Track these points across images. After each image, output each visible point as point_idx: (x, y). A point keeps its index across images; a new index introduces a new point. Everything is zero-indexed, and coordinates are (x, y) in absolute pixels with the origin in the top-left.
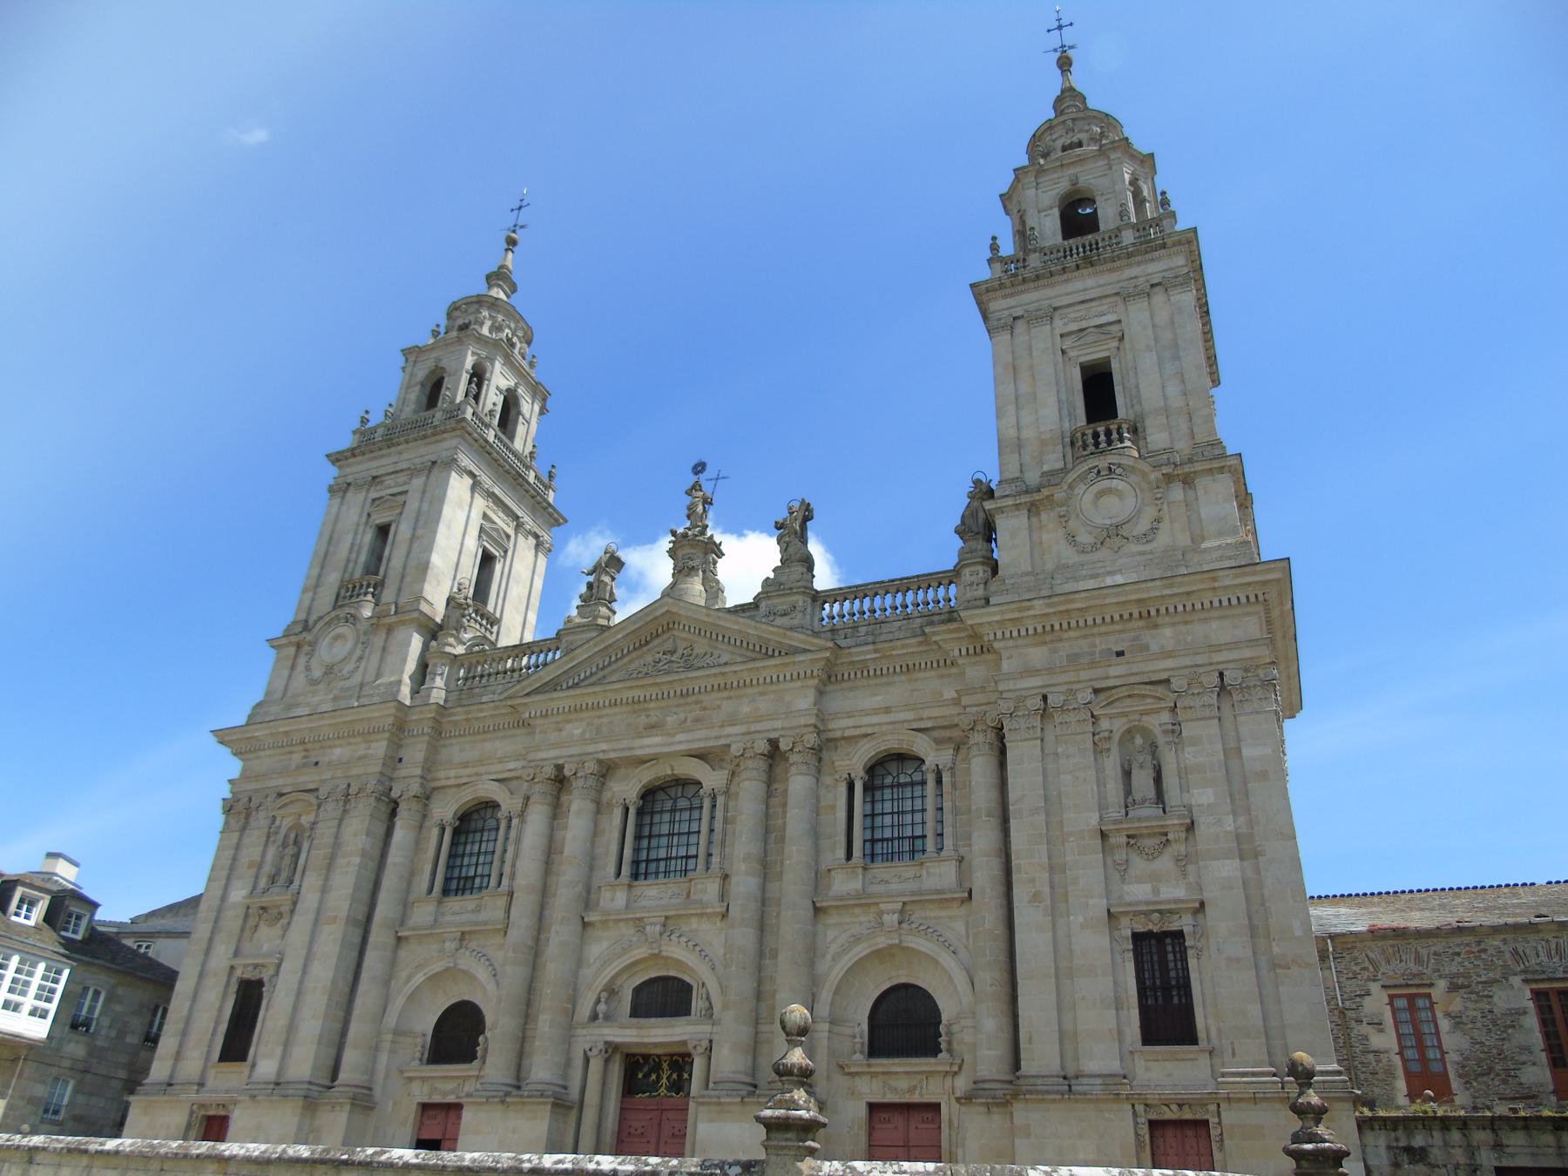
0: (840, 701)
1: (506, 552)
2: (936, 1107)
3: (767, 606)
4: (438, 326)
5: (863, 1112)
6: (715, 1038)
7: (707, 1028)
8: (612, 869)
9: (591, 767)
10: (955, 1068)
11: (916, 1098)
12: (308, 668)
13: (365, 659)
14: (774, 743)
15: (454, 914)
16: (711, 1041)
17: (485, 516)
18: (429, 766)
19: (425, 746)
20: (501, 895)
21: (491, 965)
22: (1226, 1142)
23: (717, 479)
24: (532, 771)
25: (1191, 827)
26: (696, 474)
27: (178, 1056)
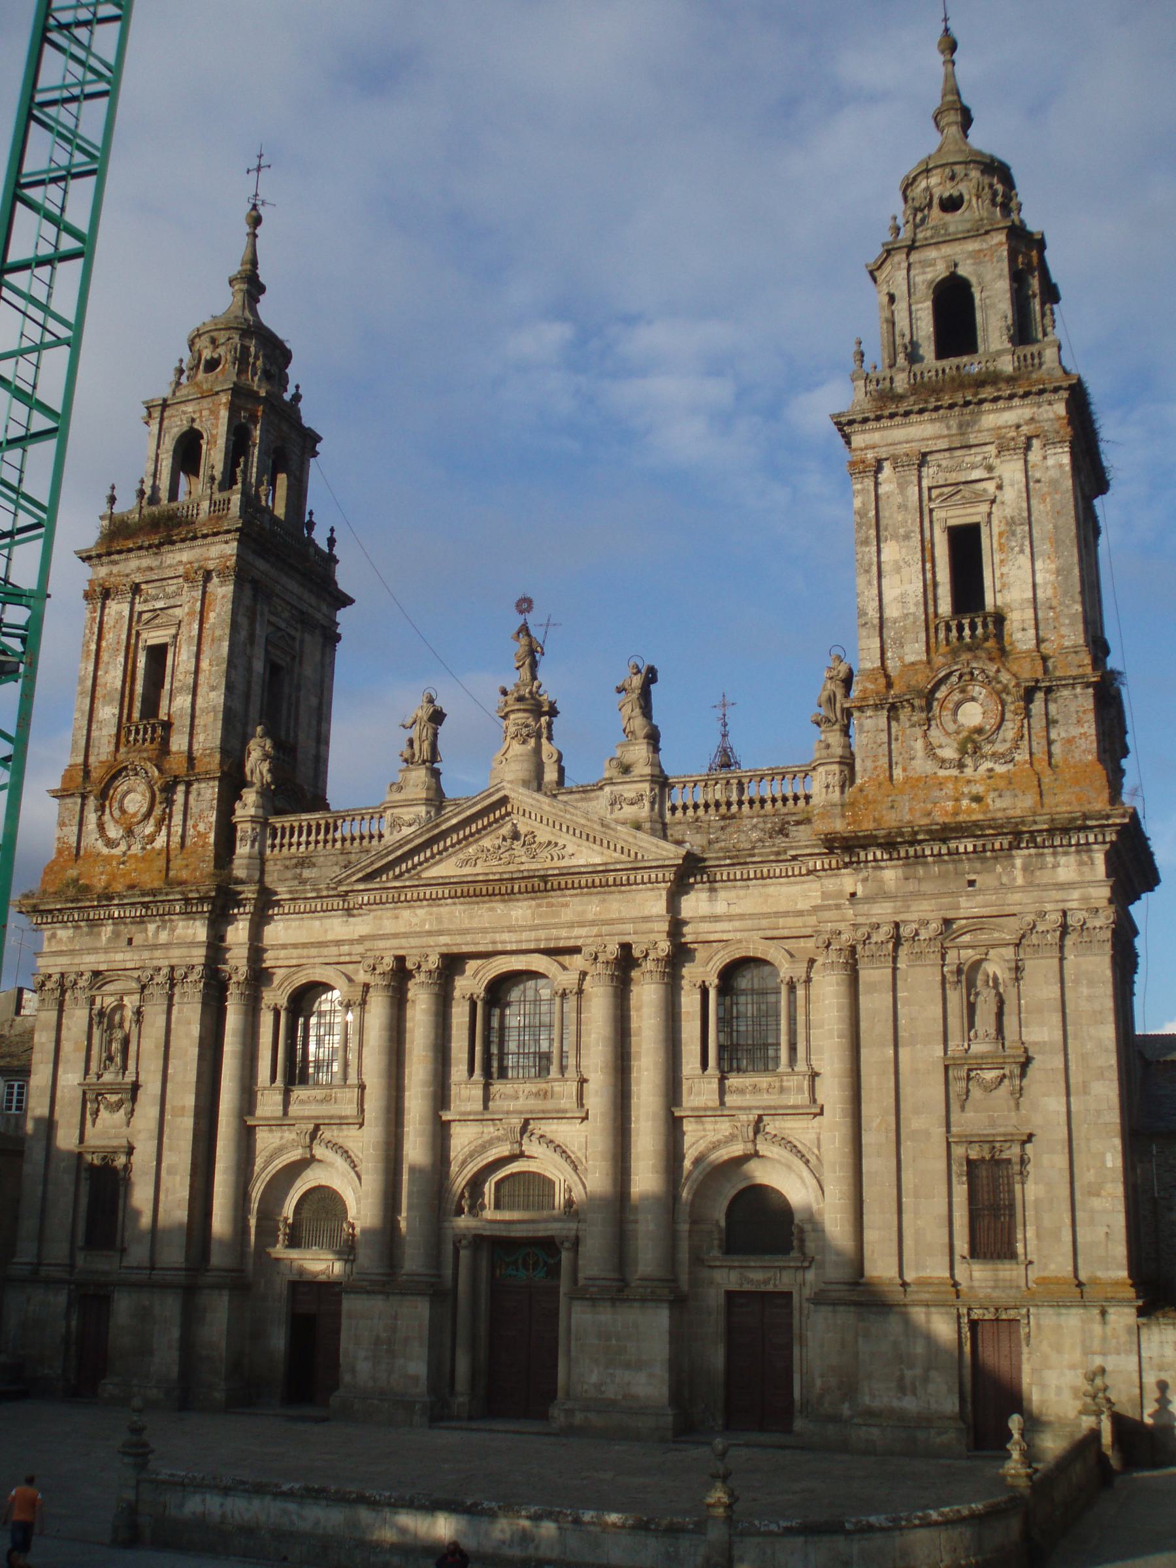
0: (694, 904)
1: (293, 658)
2: (790, 1294)
3: (612, 793)
4: (181, 361)
5: (722, 1300)
6: (580, 1234)
7: (574, 1226)
8: (464, 1067)
9: (433, 962)
10: (806, 1264)
11: (770, 1288)
12: (101, 827)
13: (166, 822)
14: (626, 947)
15: (302, 1102)
16: (577, 1238)
17: (270, 623)
18: (256, 951)
19: (247, 924)
20: (349, 1086)
21: (349, 1157)
22: (1032, 1341)
23: (548, 625)
24: (371, 962)
25: (1025, 1065)
26: (521, 612)
27: (41, 1237)
